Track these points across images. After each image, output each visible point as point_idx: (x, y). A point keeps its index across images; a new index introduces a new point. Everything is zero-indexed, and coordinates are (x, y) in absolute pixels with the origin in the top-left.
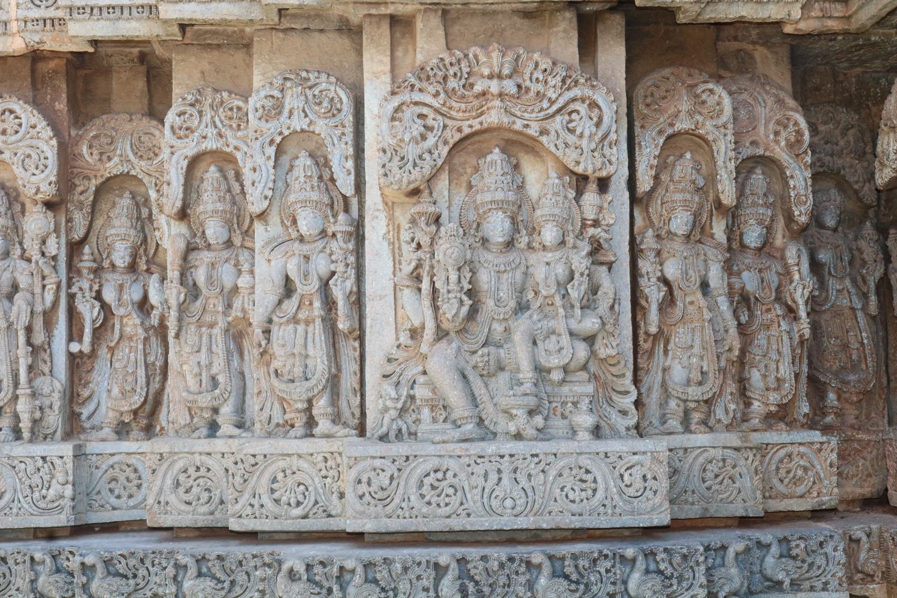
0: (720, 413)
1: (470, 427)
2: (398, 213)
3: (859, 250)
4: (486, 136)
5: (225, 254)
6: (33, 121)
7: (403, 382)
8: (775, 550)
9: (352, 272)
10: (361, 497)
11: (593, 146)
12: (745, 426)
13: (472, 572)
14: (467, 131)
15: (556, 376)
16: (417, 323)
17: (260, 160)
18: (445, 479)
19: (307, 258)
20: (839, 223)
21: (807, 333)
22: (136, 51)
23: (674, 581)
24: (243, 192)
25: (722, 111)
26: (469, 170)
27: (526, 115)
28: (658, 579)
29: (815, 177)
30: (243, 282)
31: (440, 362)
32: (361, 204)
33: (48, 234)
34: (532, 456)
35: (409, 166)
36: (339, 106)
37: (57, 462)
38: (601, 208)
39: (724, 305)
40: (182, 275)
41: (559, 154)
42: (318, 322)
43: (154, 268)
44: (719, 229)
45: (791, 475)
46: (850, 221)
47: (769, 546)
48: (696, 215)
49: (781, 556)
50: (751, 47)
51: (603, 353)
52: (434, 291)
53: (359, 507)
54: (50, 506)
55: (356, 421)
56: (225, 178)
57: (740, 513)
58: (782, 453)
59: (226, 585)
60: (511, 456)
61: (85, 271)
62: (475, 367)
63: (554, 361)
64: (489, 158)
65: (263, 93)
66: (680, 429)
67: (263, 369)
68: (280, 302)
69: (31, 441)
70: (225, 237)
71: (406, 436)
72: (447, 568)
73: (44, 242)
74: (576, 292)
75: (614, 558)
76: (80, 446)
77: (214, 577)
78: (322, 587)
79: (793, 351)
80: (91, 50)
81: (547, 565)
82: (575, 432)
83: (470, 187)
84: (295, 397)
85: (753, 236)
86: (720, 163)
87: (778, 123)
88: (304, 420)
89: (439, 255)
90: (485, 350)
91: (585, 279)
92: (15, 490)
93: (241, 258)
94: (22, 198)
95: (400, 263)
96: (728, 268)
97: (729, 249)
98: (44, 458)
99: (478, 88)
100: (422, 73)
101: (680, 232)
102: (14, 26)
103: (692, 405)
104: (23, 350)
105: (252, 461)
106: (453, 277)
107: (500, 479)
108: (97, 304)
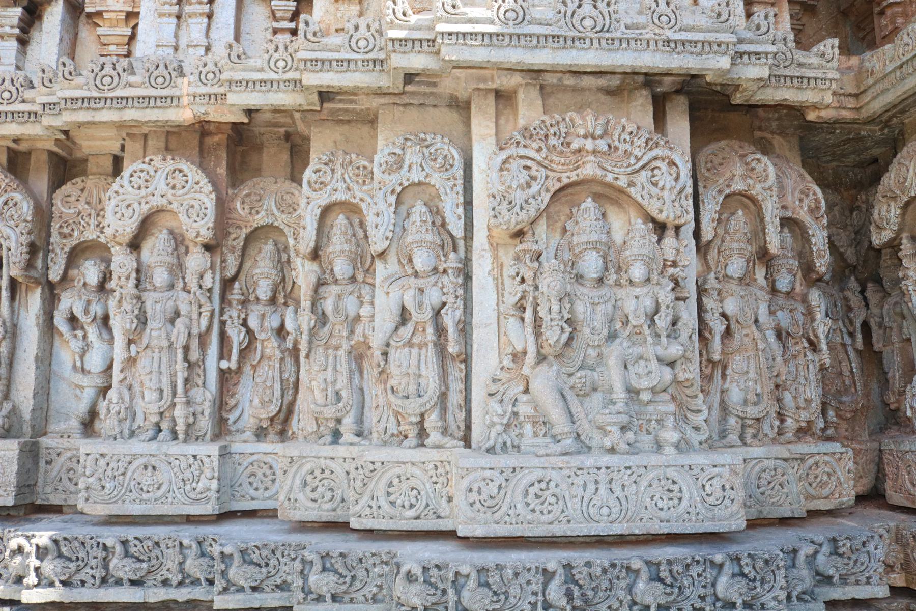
0: (767, 429)
1: (569, 441)
2: (501, 253)
4: (578, 189)
5: (350, 288)
6: (197, 178)
7: (506, 400)
9: (460, 303)
10: (472, 505)
13: (577, 577)
14: (566, 181)
15: (645, 396)
17: (382, 206)
18: (548, 489)
19: (421, 291)
22: (282, 130)
23: (758, 584)
24: (366, 237)
25: (767, 176)
26: (563, 218)
28: (744, 582)
30: (365, 311)
31: (544, 381)
32: (468, 248)
34: (626, 468)
36: (451, 162)
38: (678, 251)
40: (313, 304)
41: (644, 203)
42: (431, 346)
43: (290, 302)
45: (818, 480)
49: (831, 554)
50: (769, 136)
53: (470, 514)
54: (199, 497)
55: (462, 433)
56: (351, 225)
59: (348, 580)
60: (607, 468)
61: (234, 303)
62: (572, 388)
63: (645, 383)
64: (583, 206)
65: (387, 151)
67: (381, 386)
68: (397, 329)
69: (185, 441)
70: (350, 273)
71: (510, 449)
72: (554, 573)
73: (201, 277)
74: (662, 322)
75: (705, 563)
76: (225, 447)
77: (336, 572)
78: (436, 588)
80: (246, 121)
84: (410, 411)
85: (783, 282)
86: (768, 219)
88: (417, 432)
89: (543, 287)
91: (670, 311)
92: (171, 482)
93: (363, 292)
94: (187, 242)
95: (503, 296)
98: (195, 457)
99: (575, 145)
100: (527, 133)
101: (736, 276)
102: (185, 101)
103: (750, 422)
104: (180, 365)
105: (371, 467)
106: (555, 307)
107: (597, 489)
108: (243, 330)
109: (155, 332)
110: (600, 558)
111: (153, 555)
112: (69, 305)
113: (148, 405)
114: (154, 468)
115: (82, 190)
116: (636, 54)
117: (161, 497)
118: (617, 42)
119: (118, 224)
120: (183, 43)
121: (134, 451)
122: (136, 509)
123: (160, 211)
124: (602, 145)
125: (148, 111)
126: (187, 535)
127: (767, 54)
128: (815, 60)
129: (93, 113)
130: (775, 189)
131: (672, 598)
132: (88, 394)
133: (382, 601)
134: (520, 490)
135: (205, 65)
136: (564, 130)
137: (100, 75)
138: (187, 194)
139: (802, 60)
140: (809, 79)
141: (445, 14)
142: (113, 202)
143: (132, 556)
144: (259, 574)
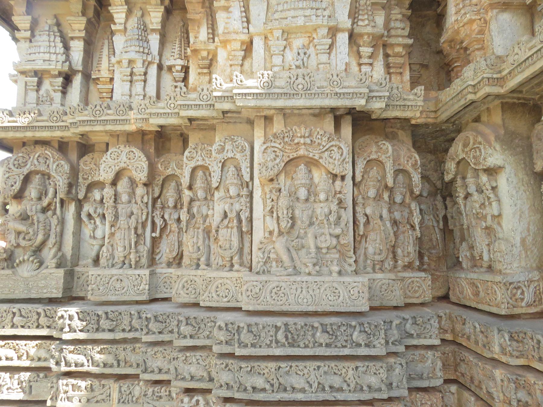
0: (386, 265)
2: (266, 188)
3: (435, 205)
4: (299, 159)
5: (204, 203)
6: (140, 155)
7: (266, 251)
8: (410, 321)
9: (248, 210)
10: (248, 296)
11: (340, 163)
12: (396, 270)
13: (290, 329)
14: (291, 157)
15: (324, 251)
16: (272, 229)
17: (216, 168)
18: (280, 290)
19: (232, 204)
20: (428, 195)
21: (419, 235)
22: (179, 132)
23: (372, 336)
25: (388, 151)
26: (292, 172)
27: (314, 152)
29: (422, 177)
30: (210, 212)
31: (280, 245)
32: (253, 184)
33: (144, 195)
34: (315, 282)
35: (269, 170)
37: (143, 276)
38: (342, 187)
39: (388, 224)
42: (235, 228)
44: (386, 196)
45: (414, 289)
46: (433, 194)
47: (408, 320)
48: (378, 190)
49: (413, 324)
51: (342, 242)
52: (278, 217)
53: (247, 301)
55: (249, 265)
56: (205, 175)
57: (395, 305)
58: (410, 280)
59: (197, 329)
60: (306, 282)
62: (293, 246)
63: (324, 245)
64: (300, 167)
65: (218, 144)
66: (372, 271)
67: (216, 245)
68: (222, 220)
69: (135, 268)
70: (204, 196)
71: (266, 272)
72: (280, 327)
73: (143, 198)
74: (332, 219)
75: (347, 325)
76: (153, 271)
77: (192, 325)
78: (231, 333)
79: (414, 242)
80: (160, 130)
81: (320, 327)
82: (331, 273)
83: (293, 178)
84: (226, 256)
85: (398, 199)
86: (387, 171)
87: (408, 157)
88: (230, 264)
89: (280, 204)
90: (297, 240)
91: (336, 214)
93: (210, 204)
96: (390, 211)
97: (390, 204)
98: (139, 275)
99: (296, 141)
100: (275, 136)
101: (372, 197)
102: (132, 121)
103: (376, 262)
105: (209, 280)
106: (285, 212)
107: (302, 291)
108: (162, 220)
109: (122, 222)
110: (300, 321)
111: (118, 318)
113: (119, 253)
114: (121, 280)
115: (92, 159)
116: (321, 100)
117: (124, 293)
118: (313, 95)
119: (105, 174)
120: (134, 93)
121: (113, 273)
122: (113, 298)
123: (124, 169)
124: (308, 141)
125: (116, 126)
126: (133, 309)
127: (384, 97)
128: (411, 97)
129: (93, 127)
130: (391, 157)
131: (332, 340)
132: (96, 248)
133: (211, 338)
134: (268, 291)
135: (141, 105)
137: (95, 110)
138: (137, 163)
139: (405, 97)
140: (408, 106)
141: (237, 85)
142: (103, 166)
143: (110, 319)
144: (162, 326)
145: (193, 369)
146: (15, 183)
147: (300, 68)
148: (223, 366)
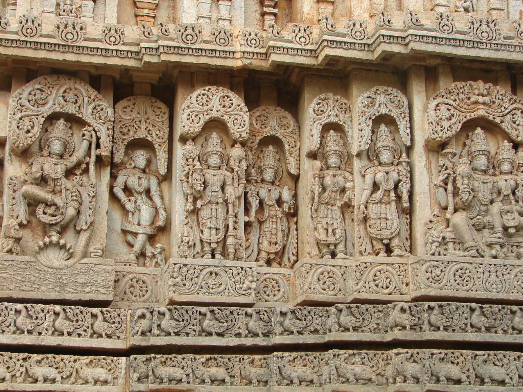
9: (409, 181)
10: (428, 279)
13: (486, 313)
18: (465, 273)
19: (387, 173)
30: (349, 185)
34: (505, 266)
35: (445, 130)
36: (402, 104)
54: (244, 292)
59: (361, 319)
60: (495, 265)
64: (476, 132)
92: (227, 283)
95: (432, 179)
98: (242, 268)
99: (473, 99)
112: (124, 180)
117: (220, 292)
124: (487, 99)
129: (180, 57)
136: (467, 91)
137: (185, 34)
144: (302, 324)
145: (358, 369)
146: (33, 127)
147: (469, 12)
148: (409, 355)
